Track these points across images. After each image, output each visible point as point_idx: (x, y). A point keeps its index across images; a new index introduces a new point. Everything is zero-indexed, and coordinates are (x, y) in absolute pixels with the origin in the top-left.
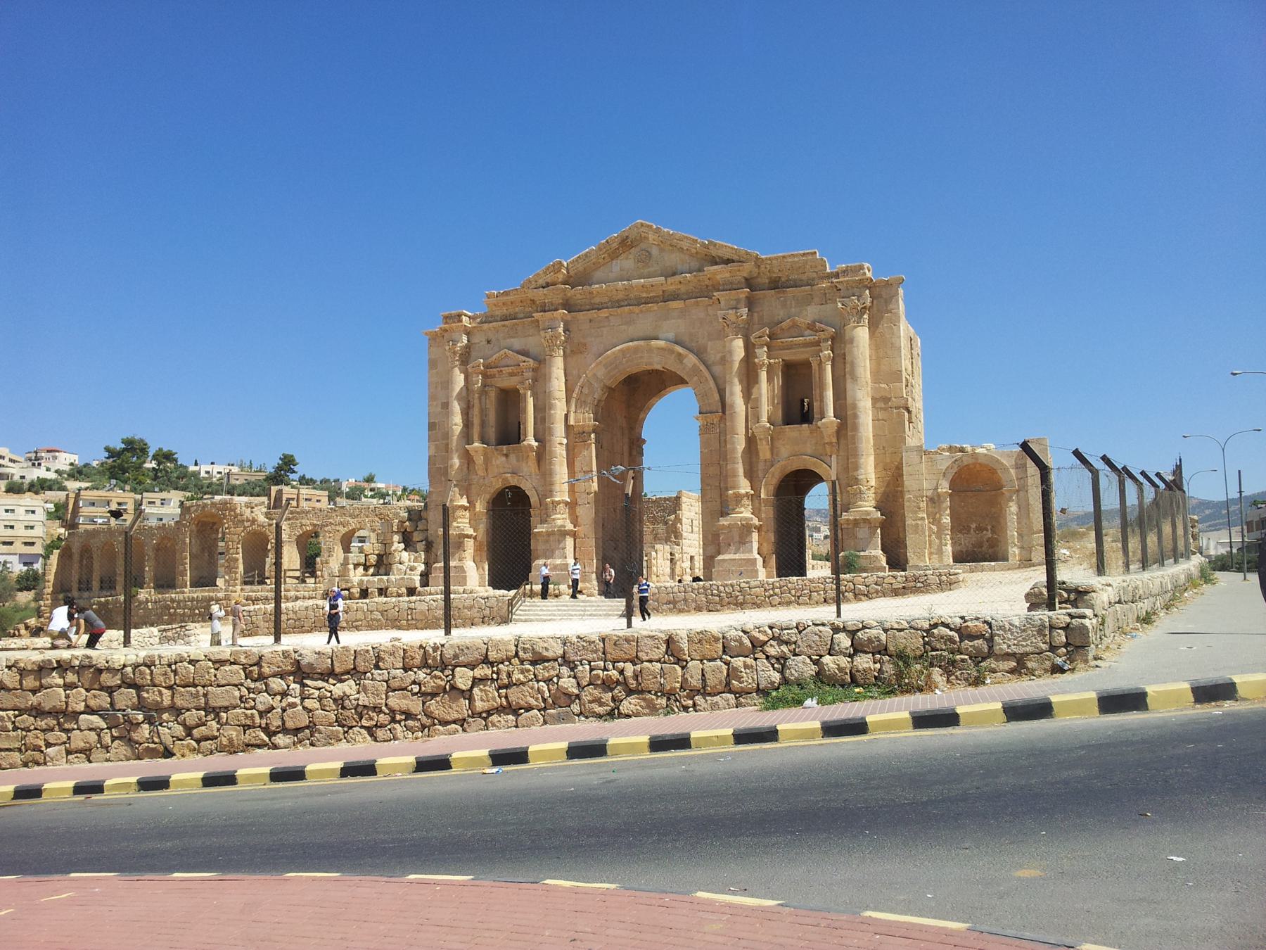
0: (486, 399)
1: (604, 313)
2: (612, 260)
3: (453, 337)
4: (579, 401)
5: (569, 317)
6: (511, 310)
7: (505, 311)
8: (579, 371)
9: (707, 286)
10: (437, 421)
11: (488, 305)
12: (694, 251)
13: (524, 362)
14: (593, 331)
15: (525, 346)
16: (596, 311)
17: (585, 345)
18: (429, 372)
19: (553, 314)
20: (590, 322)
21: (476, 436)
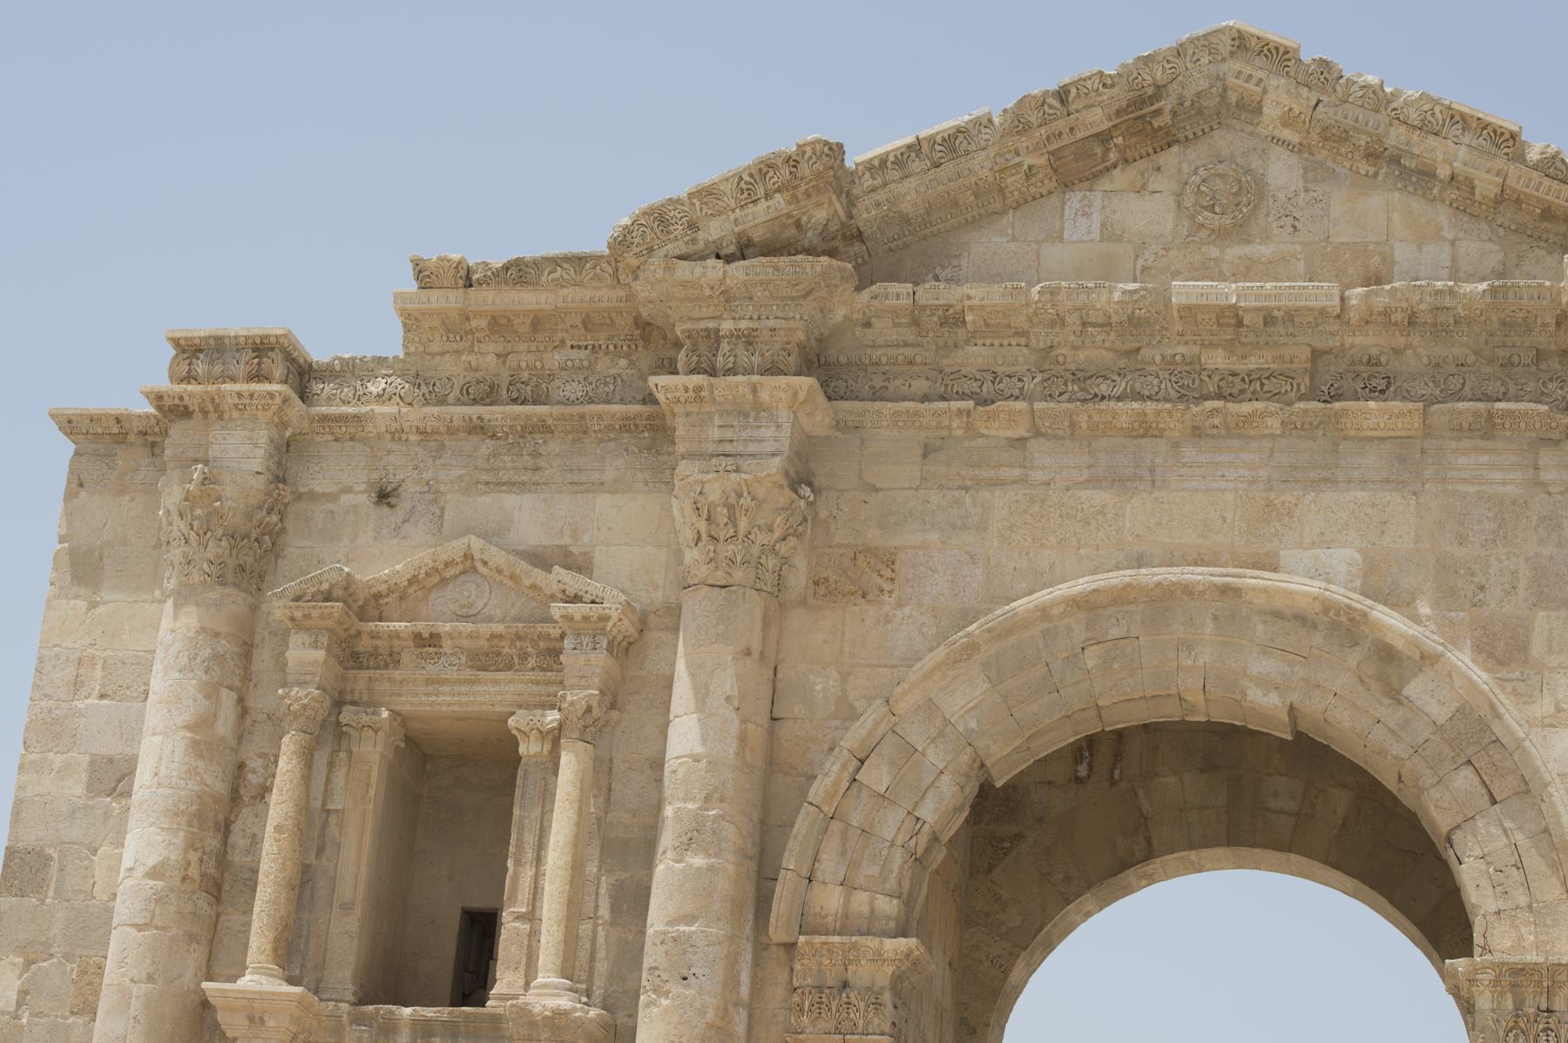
0: (331, 765)
1: (1006, 422)
2: (1066, 186)
3: (214, 451)
4: (836, 826)
5: (820, 417)
6: (523, 358)
7: (491, 359)
8: (844, 677)
9: (1540, 356)
11: (411, 321)
12: (1487, 186)
13: (576, 599)
14: (935, 498)
15: (575, 535)
16: (971, 403)
18: (49, 608)
19: (754, 390)
20: (925, 456)
21: (259, 940)
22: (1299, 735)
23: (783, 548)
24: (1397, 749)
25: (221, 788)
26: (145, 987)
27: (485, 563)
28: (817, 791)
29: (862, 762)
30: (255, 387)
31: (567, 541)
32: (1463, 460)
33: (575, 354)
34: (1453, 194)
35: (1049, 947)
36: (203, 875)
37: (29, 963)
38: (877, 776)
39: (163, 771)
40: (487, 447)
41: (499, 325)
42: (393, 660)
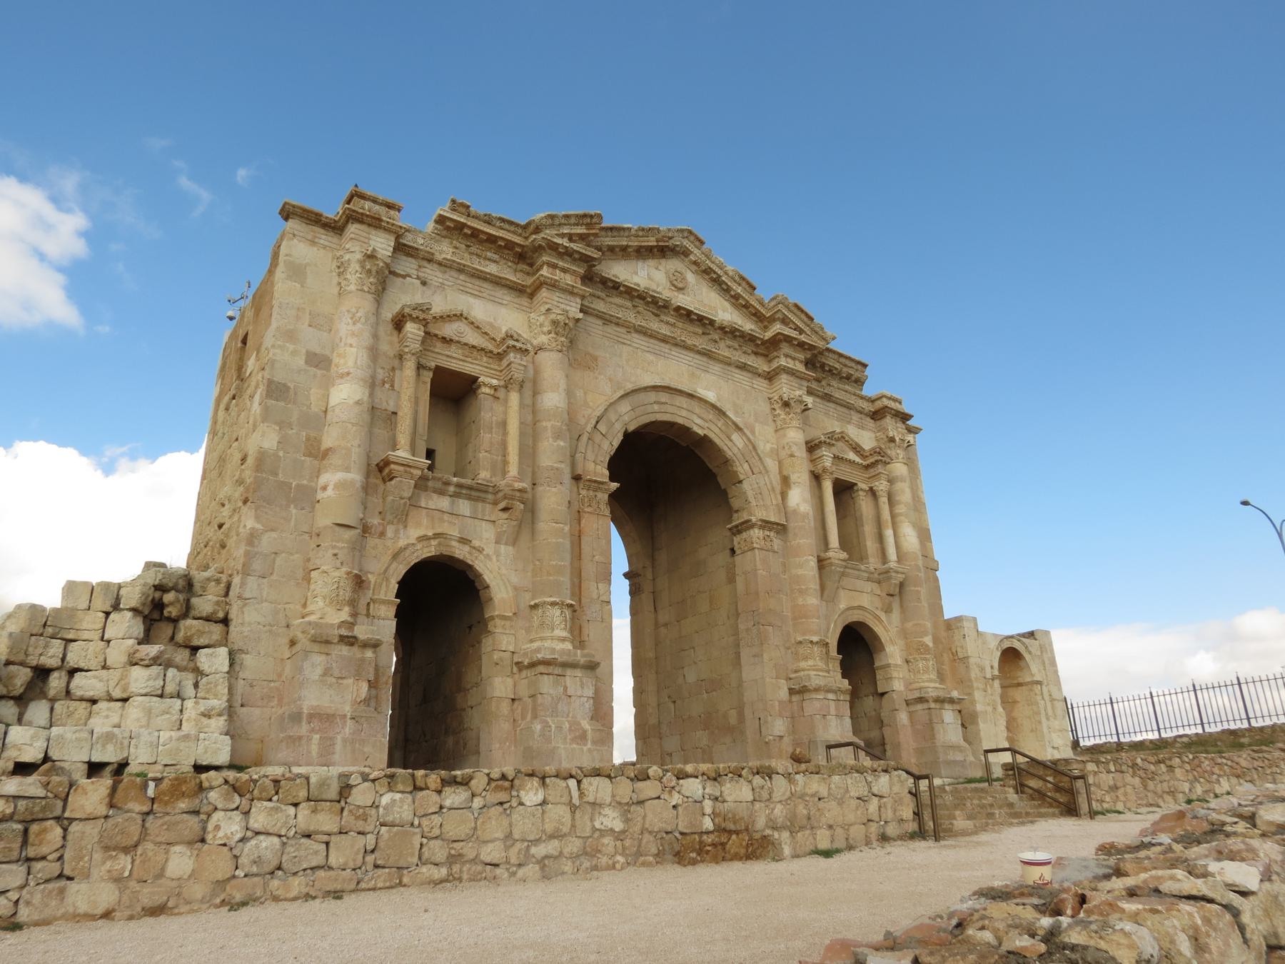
4: (590, 442)
8: (585, 393)
10: (289, 385)
11: (441, 220)
13: (517, 340)
15: (494, 319)
17: (595, 359)
24: (730, 454)
26: (357, 450)
27: (466, 318)
29: (597, 422)
31: (492, 320)
32: (736, 376)
33: (494, 255)
38: (602, 427)
39: (358, 362)
40: (462, 277)
41: (475, 234)
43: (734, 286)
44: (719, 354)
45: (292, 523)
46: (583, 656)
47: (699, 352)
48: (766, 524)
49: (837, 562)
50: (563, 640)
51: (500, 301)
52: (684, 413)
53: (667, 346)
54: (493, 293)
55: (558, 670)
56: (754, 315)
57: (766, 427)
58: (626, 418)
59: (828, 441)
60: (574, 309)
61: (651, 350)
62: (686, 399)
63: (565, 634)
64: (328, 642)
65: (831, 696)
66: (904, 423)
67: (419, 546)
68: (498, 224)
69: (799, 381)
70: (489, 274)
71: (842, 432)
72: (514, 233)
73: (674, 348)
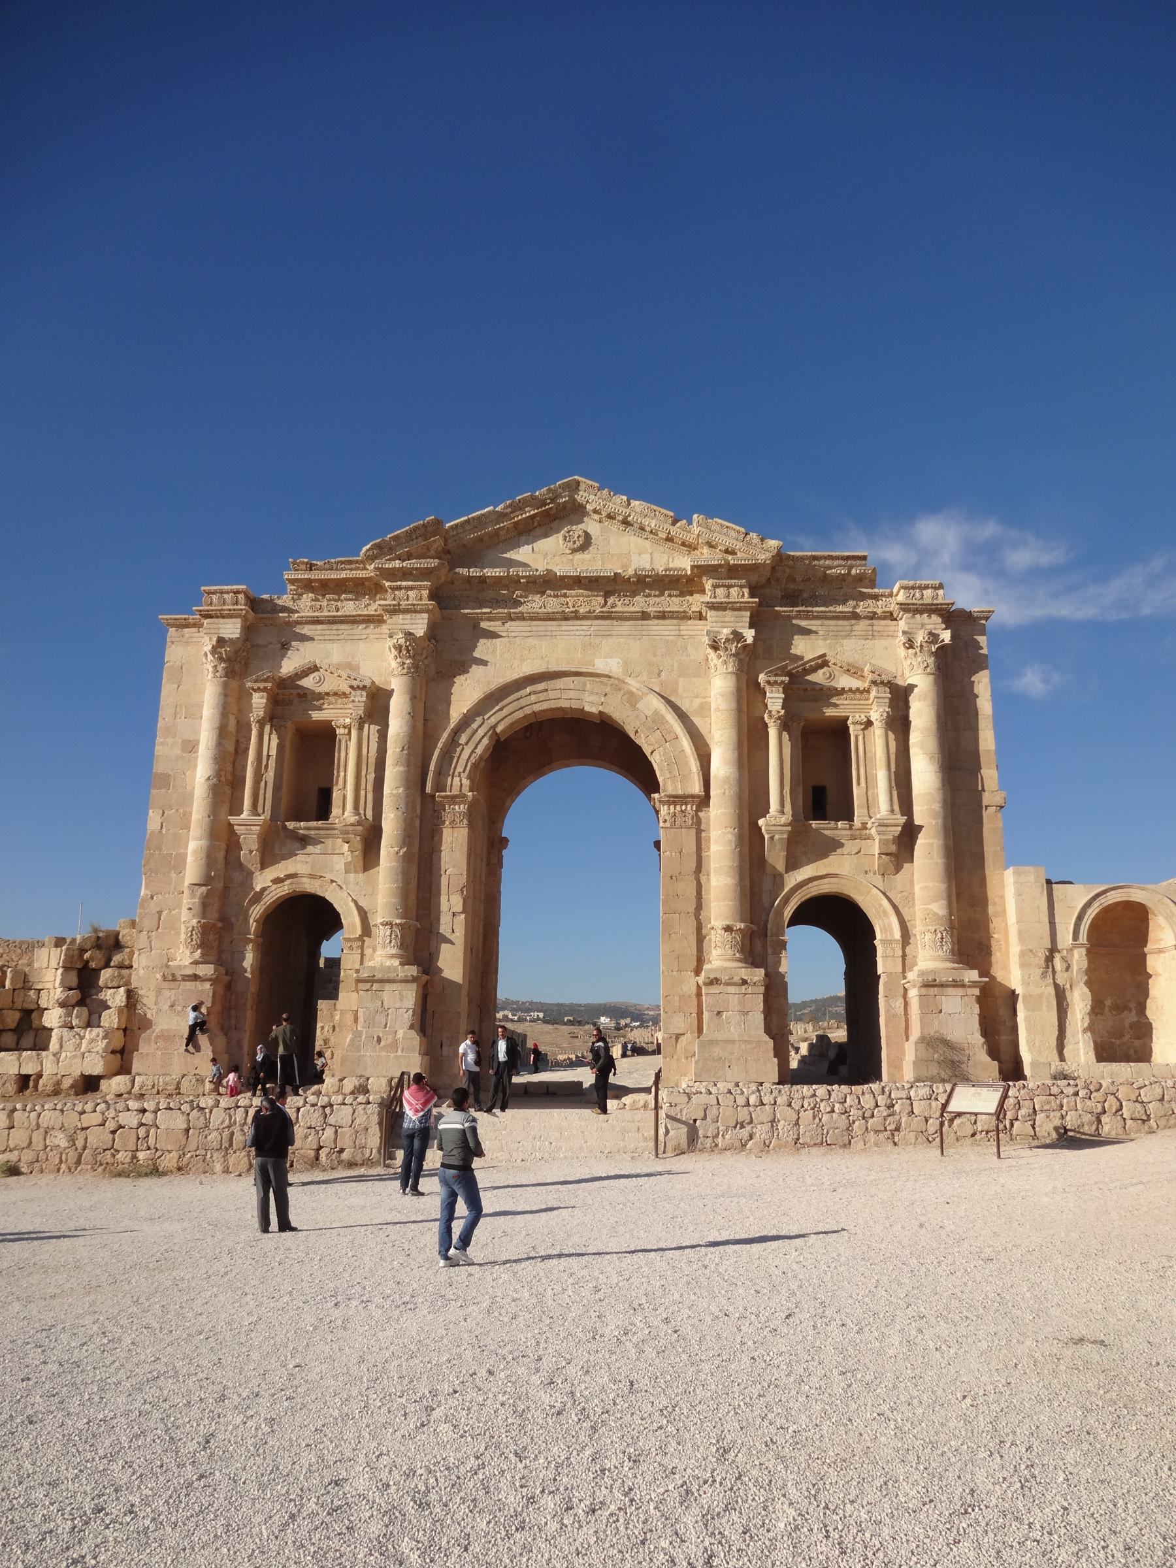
2: (520, 534)
22: (602, 721)
23: (426, 662)
25: (230, 747)
28: (440, 745)
30: (235, 607)
34: (652, 536)
35: (518, 793)
36: (226, 780)
37: (164, 813)
42: (290, 703)
43: (646, 522)
44: (623, 612)
45: (173, 886)
46: (402, 972)
47: (597, 618)
48: (676, 799)
49: (773, 828)
50: (392, 956)
51: (359, 637)
52: (571, 694)
53: (554, 623)
54: (351, 632)
55: (376, 986)
56: (683, 544)
57: (695, 680)
58: (493, 720)
59: (772, 679)
60: (420, 626)
61: (533, 633)
62: (573, 678)
63: (394, 951)
64: (174, 980)
65: (731, 989)
66: (941, 615)
67: (274, 887)
68: (339, 567)
69: (737, 613)
70: (342, 616)
71: (824, 655)
72: (357, 569)
73: (564, 623)
